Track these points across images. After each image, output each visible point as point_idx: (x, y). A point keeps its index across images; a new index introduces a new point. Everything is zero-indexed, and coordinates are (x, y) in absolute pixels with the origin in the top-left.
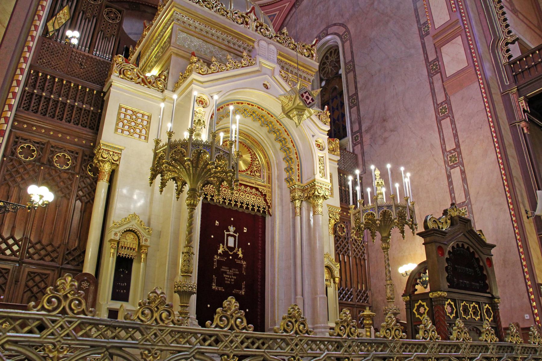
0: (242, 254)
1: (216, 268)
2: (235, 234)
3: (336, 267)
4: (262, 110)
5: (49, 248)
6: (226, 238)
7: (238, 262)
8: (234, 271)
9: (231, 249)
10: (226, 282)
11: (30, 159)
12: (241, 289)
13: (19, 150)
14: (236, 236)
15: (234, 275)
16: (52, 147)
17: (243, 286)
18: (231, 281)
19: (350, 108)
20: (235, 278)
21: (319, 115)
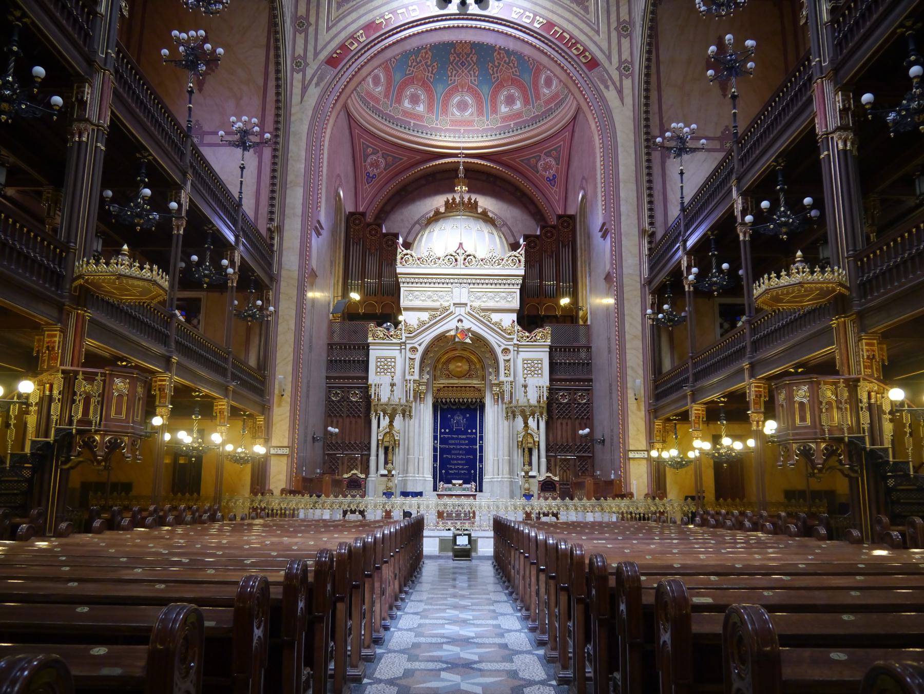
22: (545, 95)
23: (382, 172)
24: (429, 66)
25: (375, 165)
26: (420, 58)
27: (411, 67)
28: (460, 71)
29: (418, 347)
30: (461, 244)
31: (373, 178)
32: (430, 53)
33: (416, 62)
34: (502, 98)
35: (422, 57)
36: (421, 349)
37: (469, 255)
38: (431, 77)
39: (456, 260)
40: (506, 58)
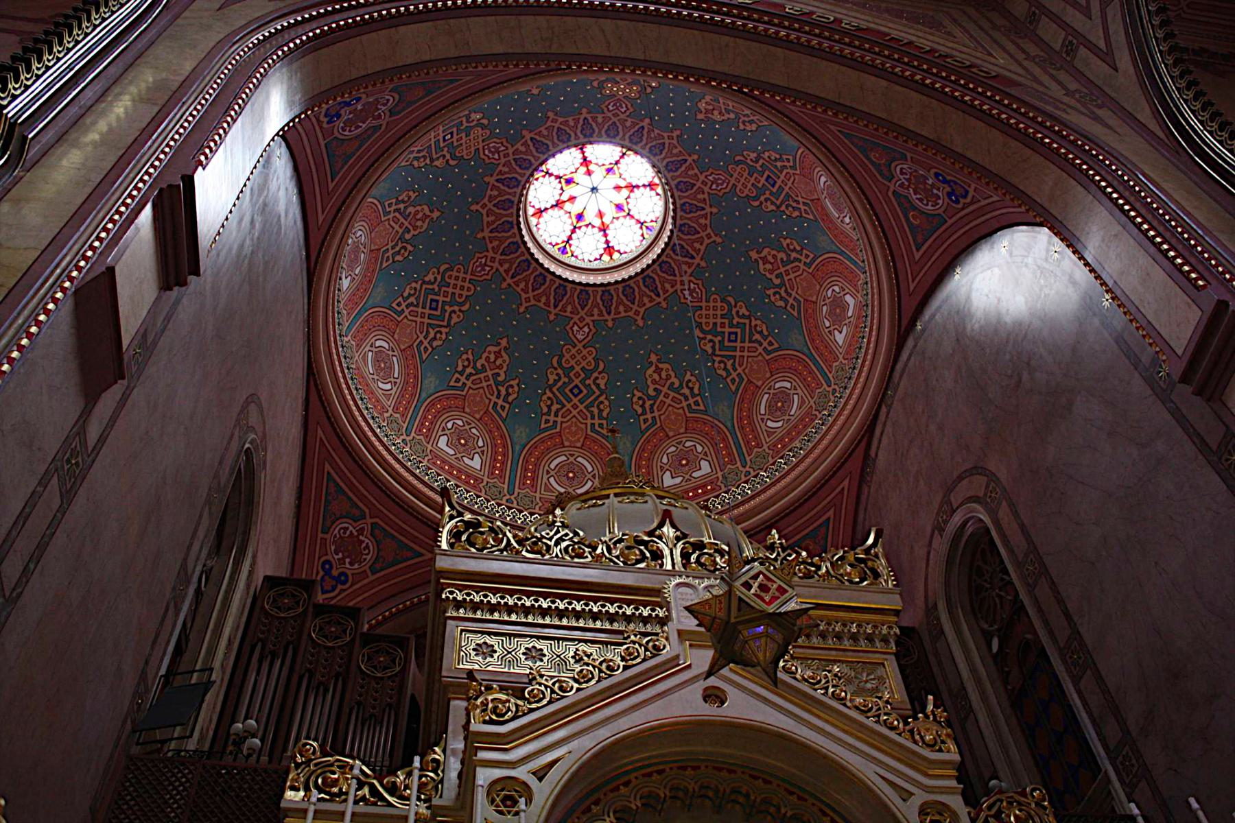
4: (730, 771)
19: (1076, 681)
21: (911, 731)
22: (769, 434)
24: (502, 383)
25: (350, 548)
26: (483, 361)
27: (461, 373)
28: (569, 406)
29: (532, 781)
30: (666, 516)
32: (506, 357)
33: (474, 367)
34: (665, 460)
35: (487, 359)
36: (543, 792)
38: (503, 408)
40: (674, 380)
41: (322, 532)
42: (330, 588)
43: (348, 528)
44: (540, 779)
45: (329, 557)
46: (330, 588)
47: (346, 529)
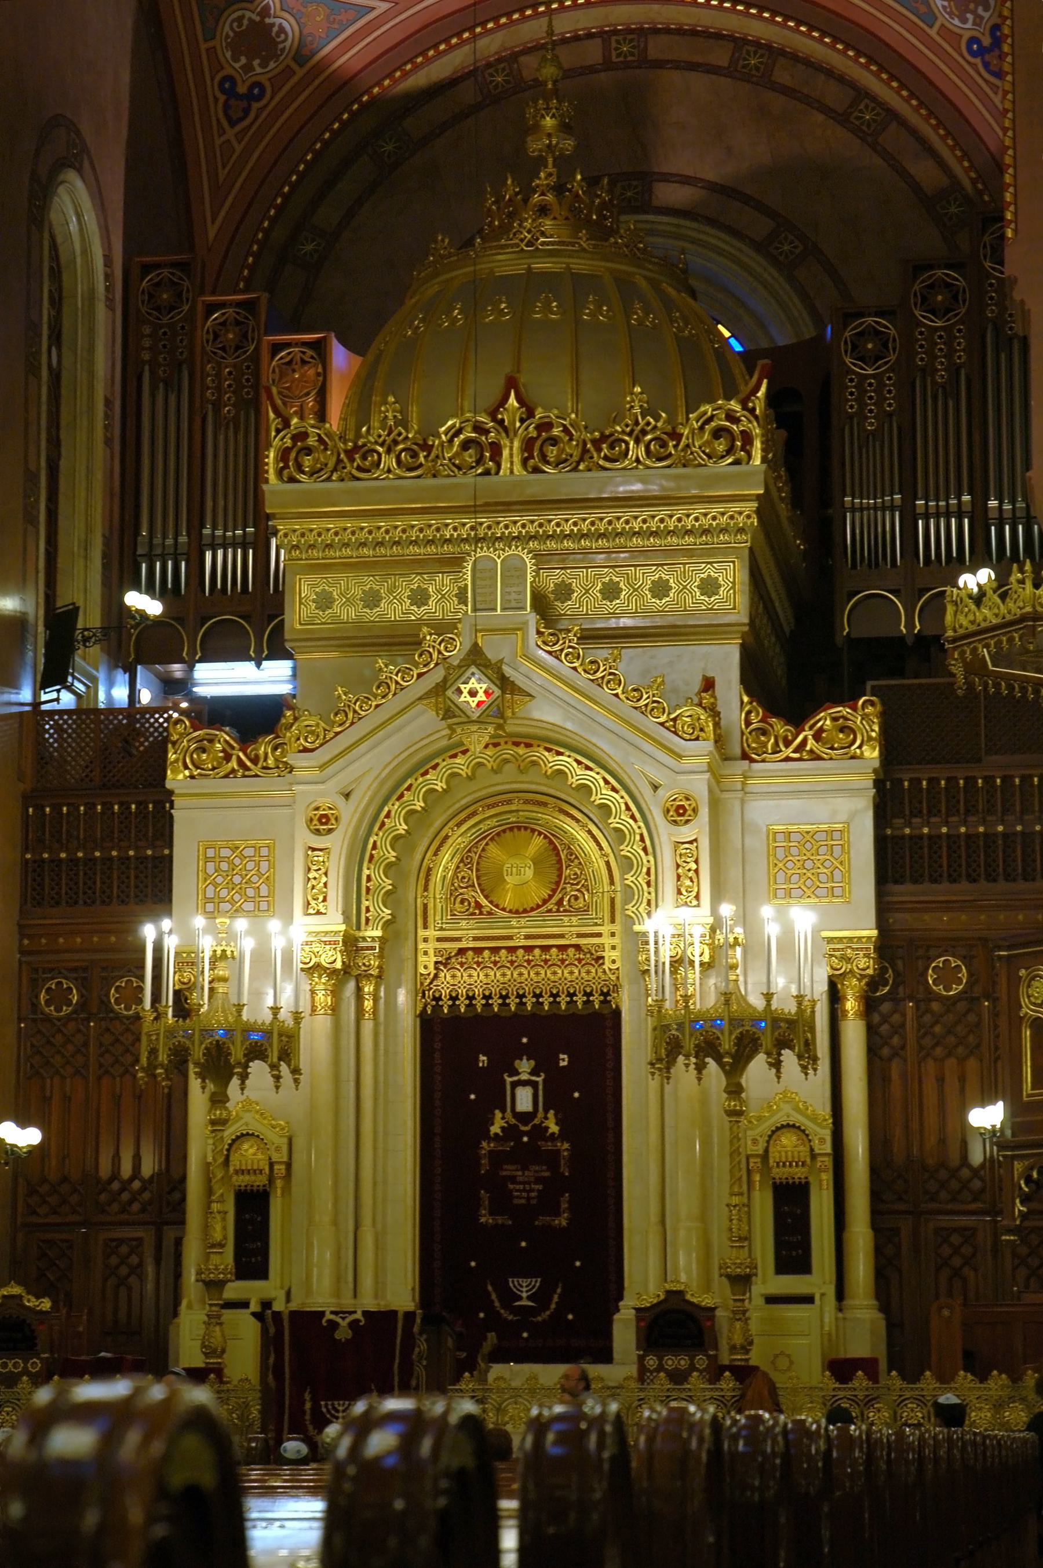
0: (557, 1124)
1: (487, 1171)
2: (534, 1078)
3: (819, 1125)
4: (528, 745)
5: (136, 1185)
6: (508, 1092)
7: (549, 1146)
8: (536, 1171)
9: (525, 1117)
10: (516, 1201)
11: (66, 1010)
12: (558, 1214)
13: (43, 996)
14: (537, 1082)
15: (538, 1180)
16: (104, 969)
17: (564, 1206)
18: (528, 1198)
20: (540, 1187)
23: (289, 72)
30: (511, 383)
31: (250, 97)
36: (349, 814)
37: (545, 426)
39: (496, 450)
41: (206, 40)
42: (241, 114)
43: (243, 17)
44: (347, 796)
45: (228, 71)
46: (241, 114)
47: (240, 19)
